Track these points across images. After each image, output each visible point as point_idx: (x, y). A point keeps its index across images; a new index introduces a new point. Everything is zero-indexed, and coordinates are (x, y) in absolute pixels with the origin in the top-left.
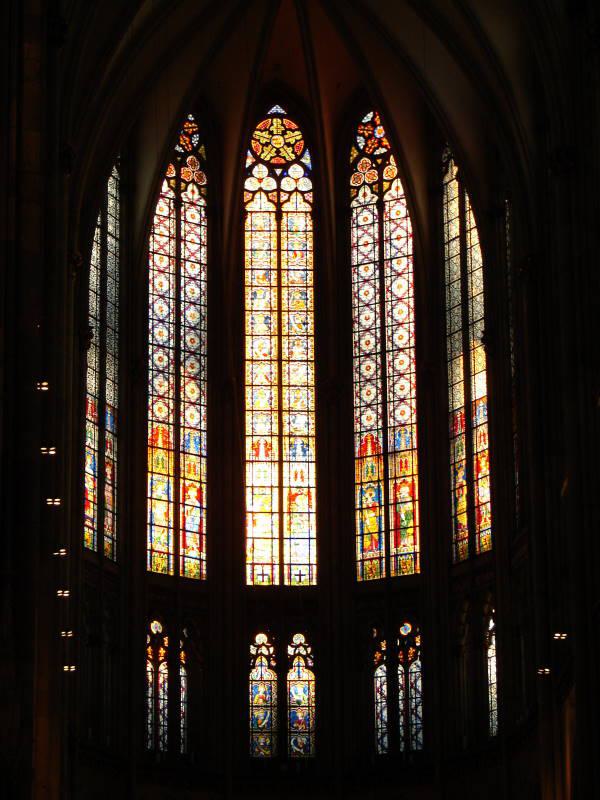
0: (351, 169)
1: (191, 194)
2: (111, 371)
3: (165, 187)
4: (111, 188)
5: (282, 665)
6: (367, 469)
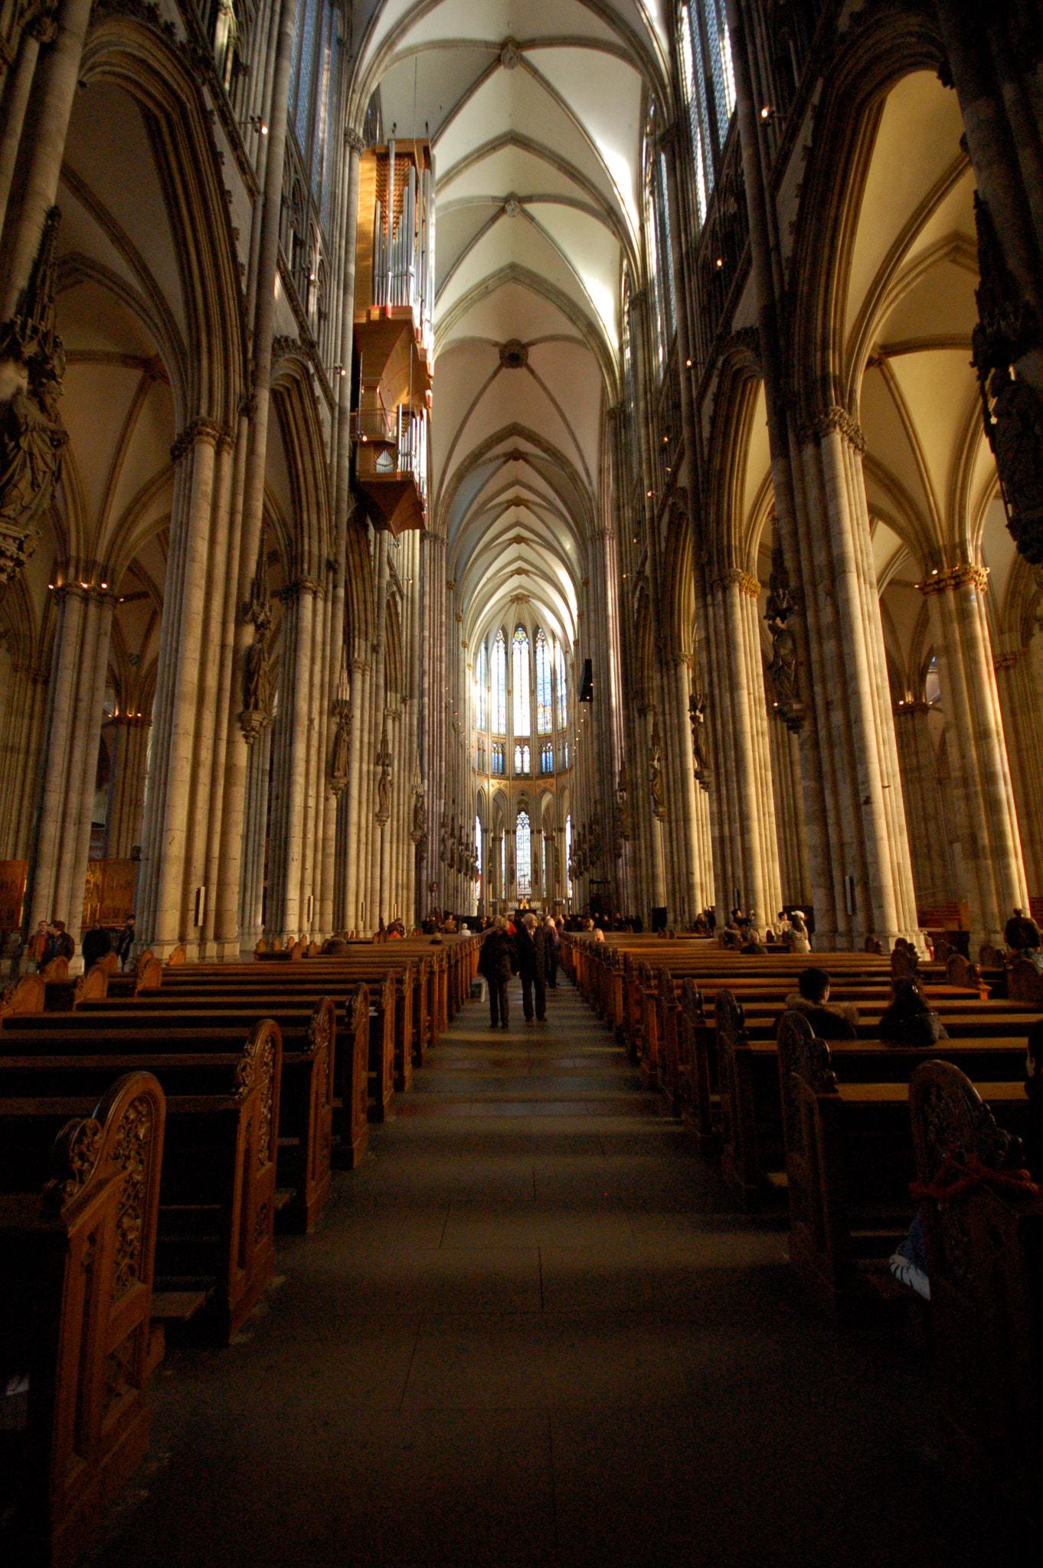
5: (522, 753)
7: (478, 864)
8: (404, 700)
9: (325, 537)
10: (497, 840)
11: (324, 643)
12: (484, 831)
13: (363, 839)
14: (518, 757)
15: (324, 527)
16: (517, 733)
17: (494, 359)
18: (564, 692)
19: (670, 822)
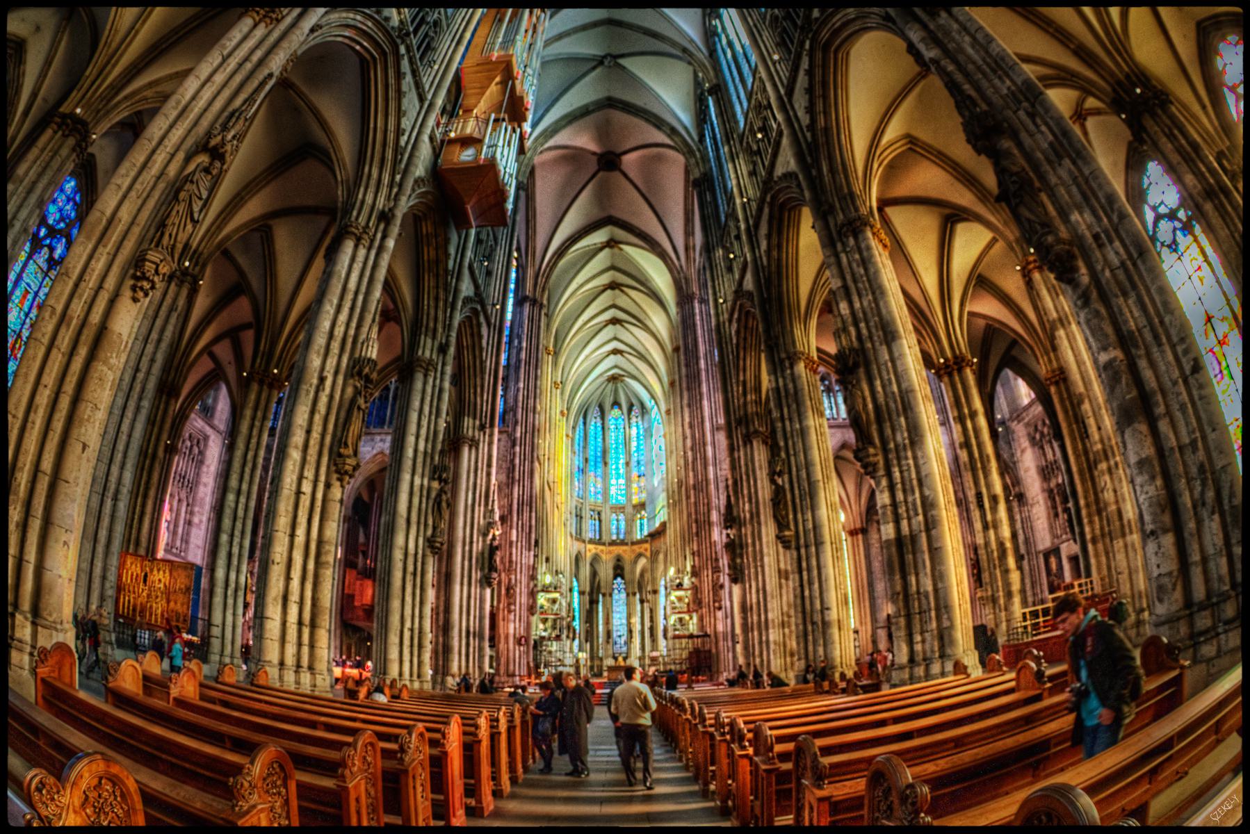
8: (482, 428)
9: (384, 191)
10: (593, 602)
11: (356, 293)
12: (581, 593)
13: (410, 568)
15: (386, 179)
17: (593, 165)
19: (798, 549)
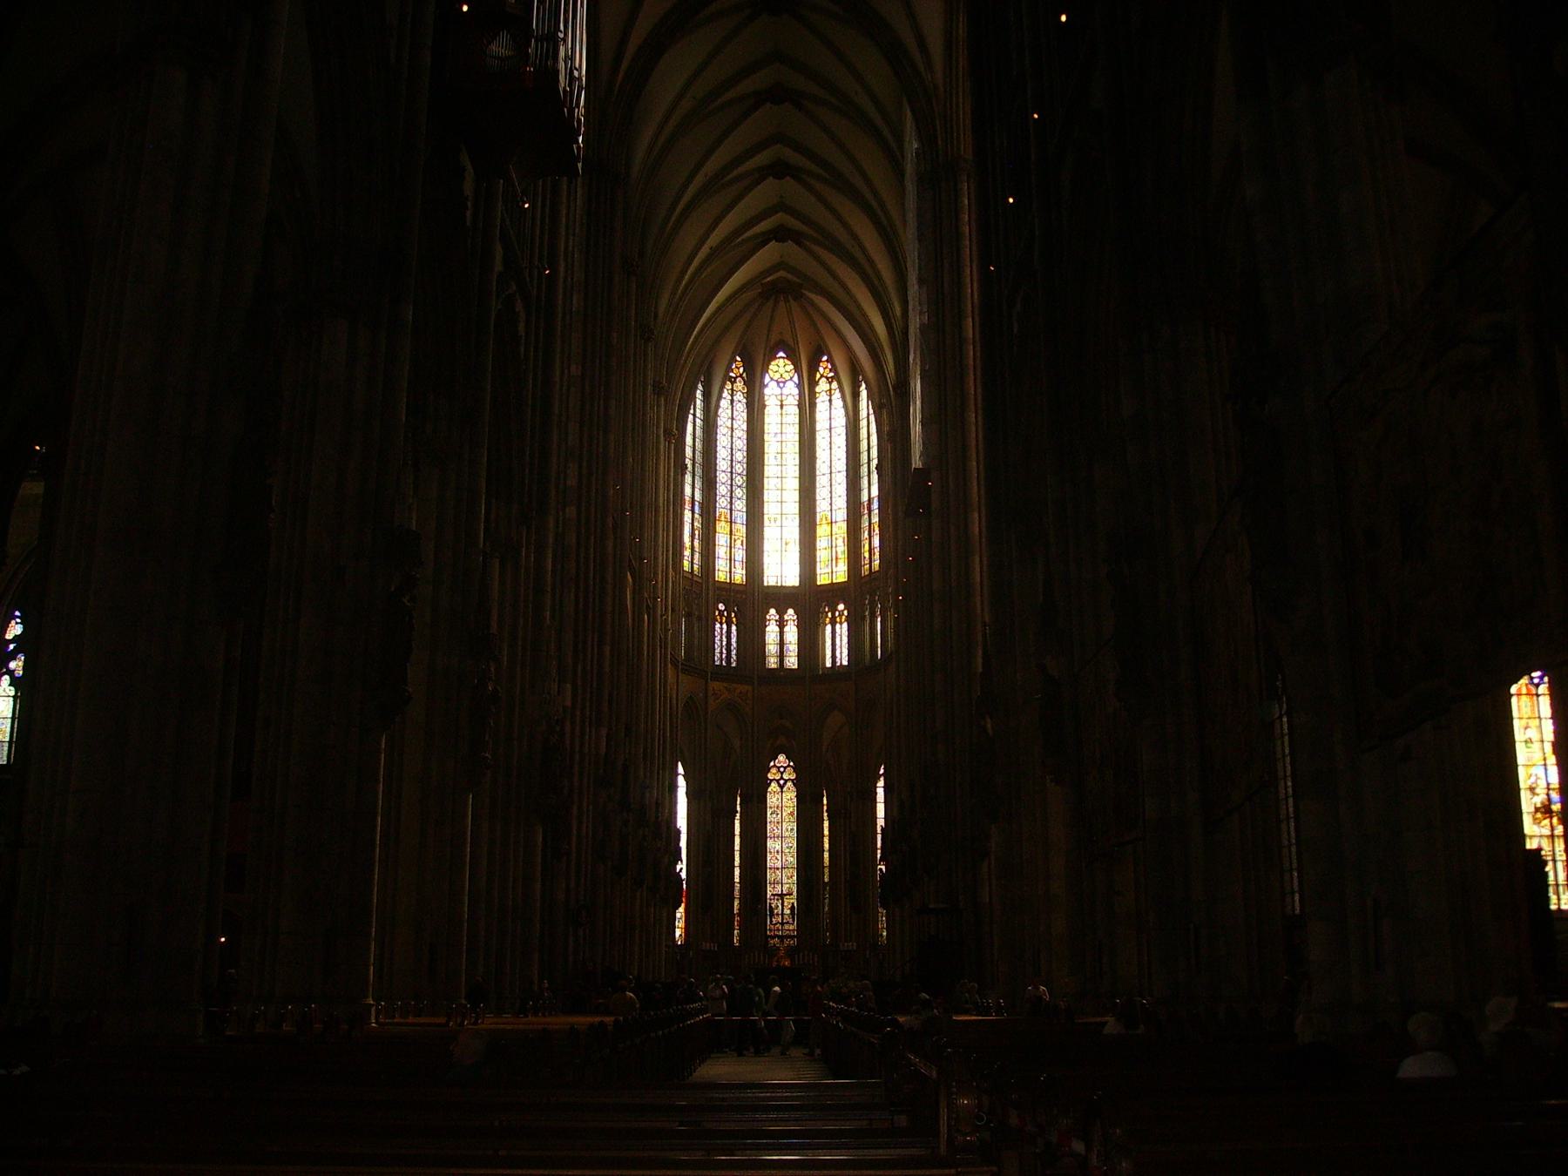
0: (817, 383)
1: (739, 397)
2: (698, 485)
3: (725, 394)
4: (699, 394)
5: (781, 624)
6: (822, 531)
7: (682, 867)
14: (772, 631)
16: (771, 578)
18: (875, 492)
